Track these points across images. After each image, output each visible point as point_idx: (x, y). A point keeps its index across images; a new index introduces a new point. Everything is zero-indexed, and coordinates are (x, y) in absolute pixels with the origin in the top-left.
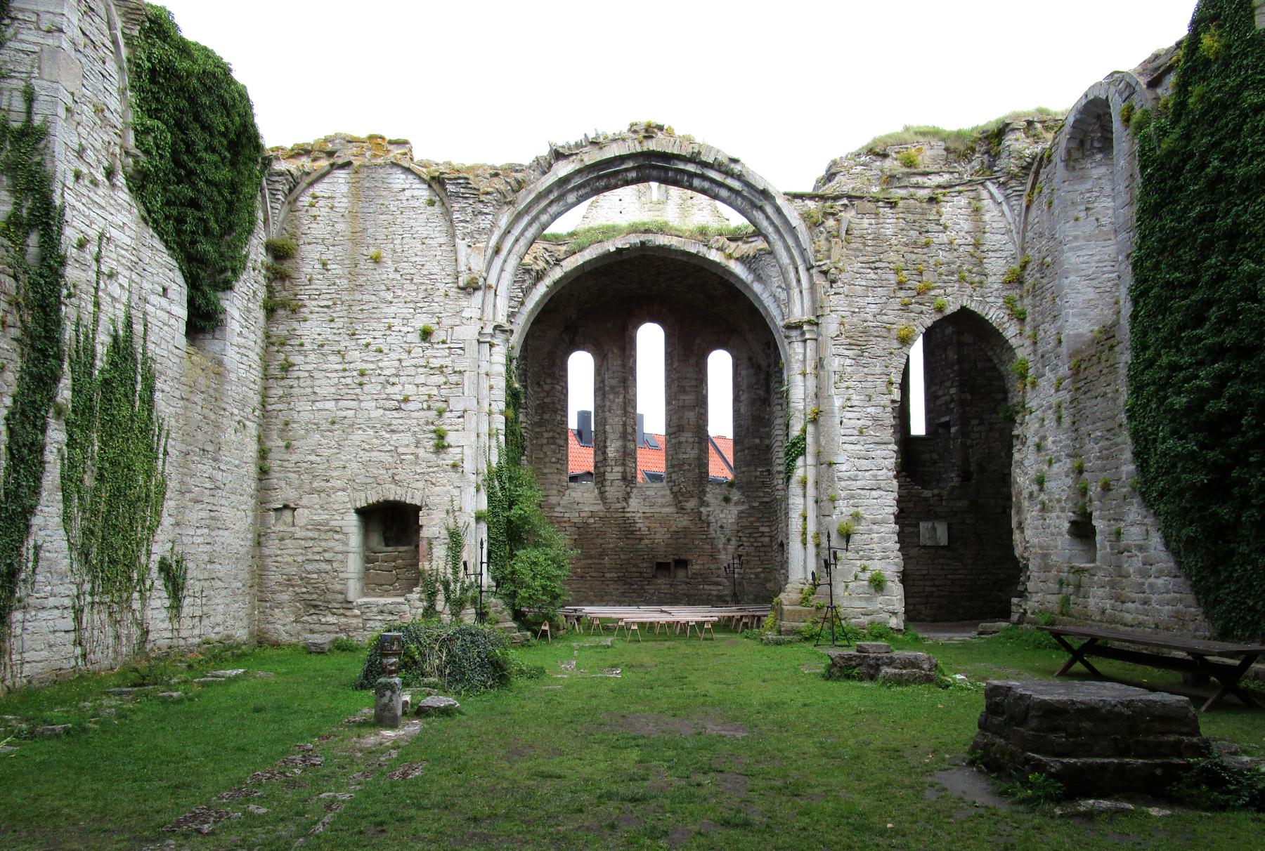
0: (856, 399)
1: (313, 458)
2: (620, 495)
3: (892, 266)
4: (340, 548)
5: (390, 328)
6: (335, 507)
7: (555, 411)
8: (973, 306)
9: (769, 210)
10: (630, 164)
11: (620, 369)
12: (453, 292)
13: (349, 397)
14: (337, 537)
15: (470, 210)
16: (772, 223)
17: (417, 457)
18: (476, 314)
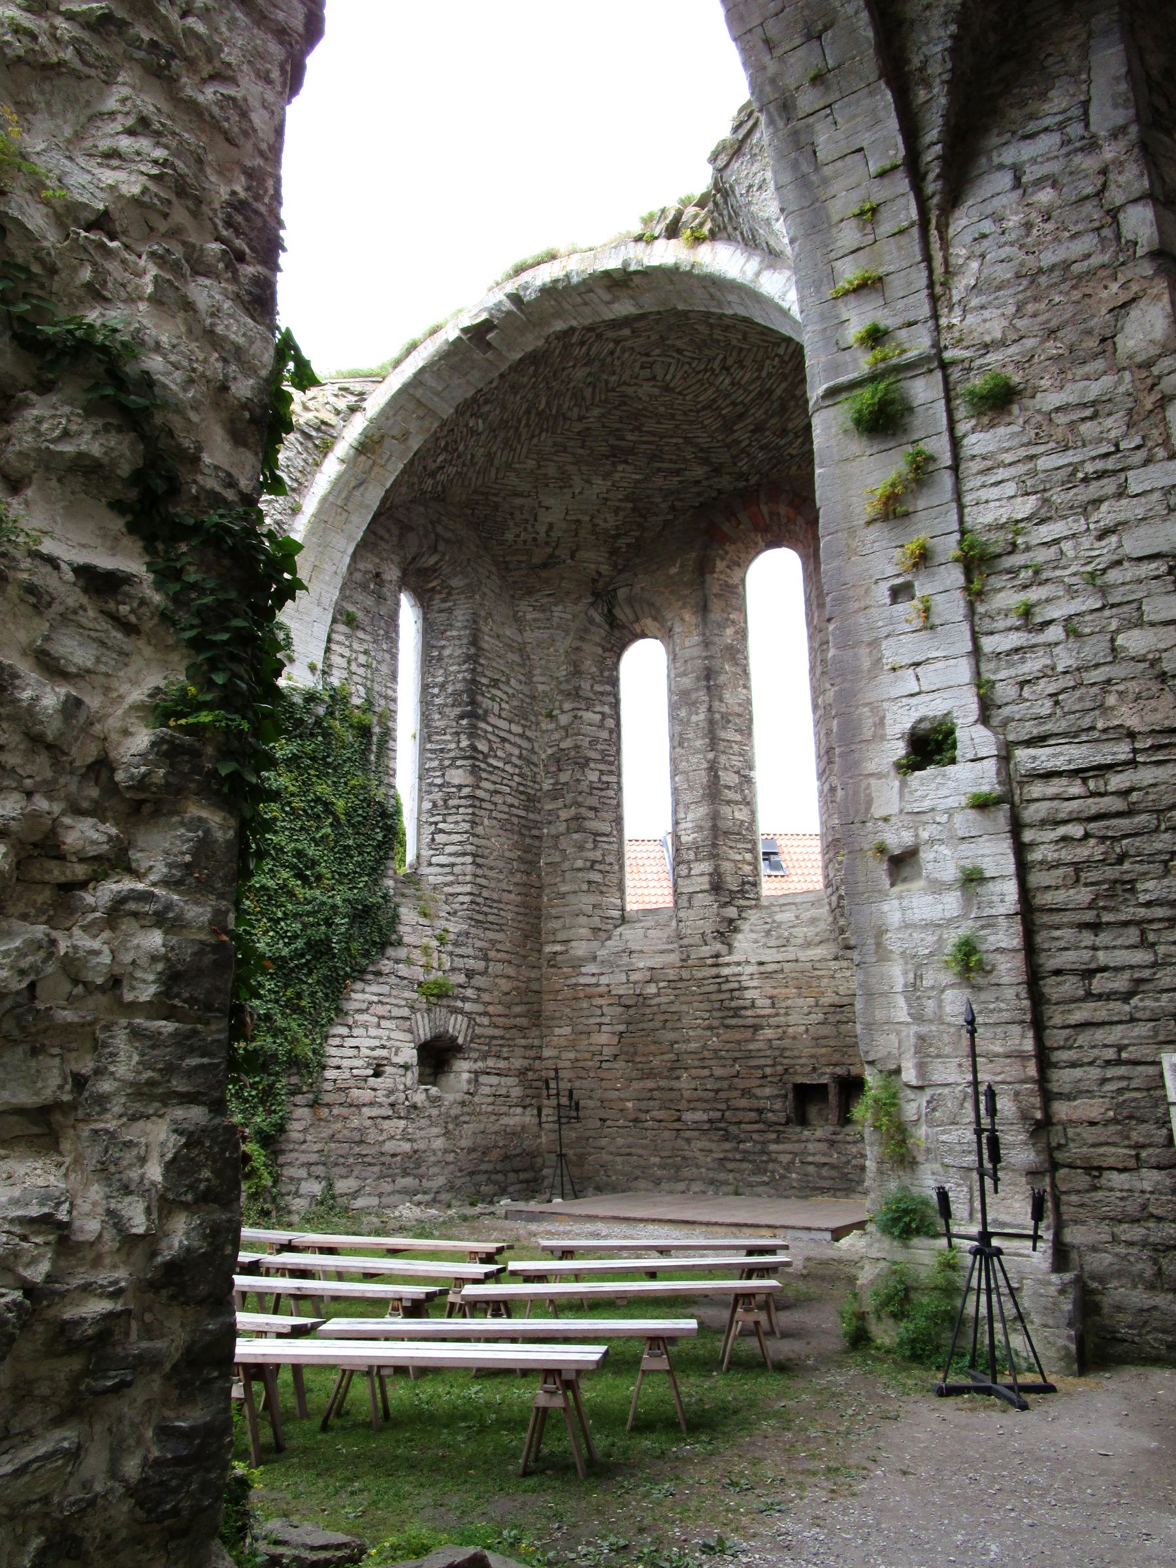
2: (708, 927)
7: (584, 764)
11: (696, 652)
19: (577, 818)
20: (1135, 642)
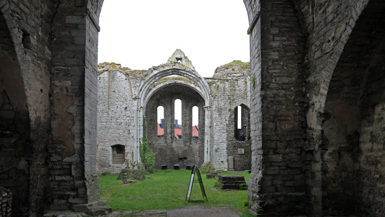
0: (219, 124)
1: (101, 135)
2: (170, 142)
3: (227, 95)
4: (108, 154)
5: (117, 107)
6: (107, 145)
8: (244, 103)
9: (201, 82)
10: (170, 71)
11: (170, 111)
12: (131, 100)
13: (109, 122)
14: (107, 152)
15: (135, 81)
16: (202, 85)
17: (124, 135)
18: (136, 104)
19: (154, 128)
20: (230, 135)
